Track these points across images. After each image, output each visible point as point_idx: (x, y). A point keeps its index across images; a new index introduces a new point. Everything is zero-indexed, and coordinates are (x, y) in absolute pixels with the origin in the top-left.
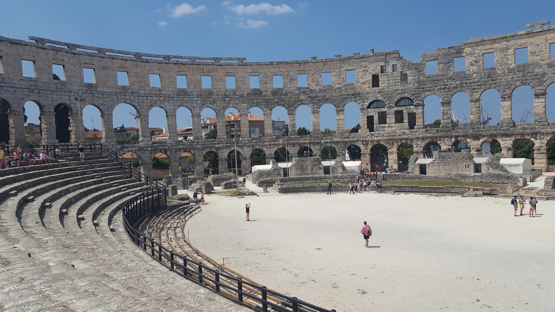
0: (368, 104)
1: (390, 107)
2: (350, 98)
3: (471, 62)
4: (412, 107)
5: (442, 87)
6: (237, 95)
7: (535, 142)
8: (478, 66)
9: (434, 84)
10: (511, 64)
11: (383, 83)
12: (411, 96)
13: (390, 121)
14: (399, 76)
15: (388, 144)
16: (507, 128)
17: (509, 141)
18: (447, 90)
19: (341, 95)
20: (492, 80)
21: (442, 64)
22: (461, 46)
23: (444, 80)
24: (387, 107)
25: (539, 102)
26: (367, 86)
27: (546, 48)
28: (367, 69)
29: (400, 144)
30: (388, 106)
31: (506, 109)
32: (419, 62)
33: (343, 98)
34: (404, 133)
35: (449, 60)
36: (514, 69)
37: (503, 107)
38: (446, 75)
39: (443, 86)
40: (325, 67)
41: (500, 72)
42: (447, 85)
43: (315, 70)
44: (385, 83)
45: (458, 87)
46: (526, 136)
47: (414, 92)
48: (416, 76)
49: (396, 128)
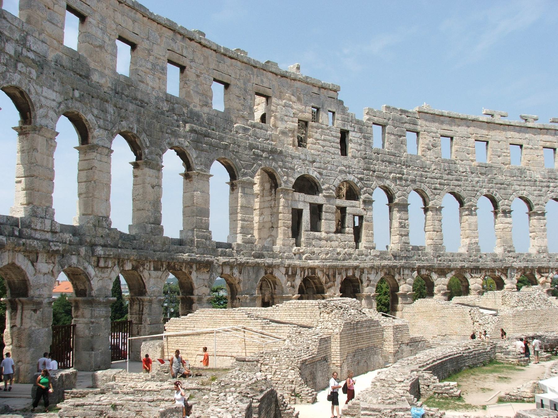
3: (428, 144)
6: (29, 50)
10: (472, 161)
11: (315, 144)
16: (476, 258)
17: (479, 279)
21: (393, 134)
24: (324, 196)
25: (507, 223)
29: (344, 277)
30: (325, 194)
33: (254, 154)
38: (398, 156)
39: (399, 174)
42: (403, 174)
43: (202, 64)
44: (319, 143)
46: (497, 272)
49: (337, 243)
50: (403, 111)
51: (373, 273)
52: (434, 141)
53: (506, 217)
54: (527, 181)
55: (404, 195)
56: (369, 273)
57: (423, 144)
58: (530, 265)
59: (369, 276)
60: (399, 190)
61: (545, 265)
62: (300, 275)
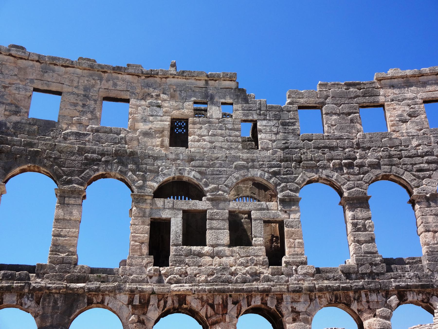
0: (156, 185)
2: (107, 162)
3: (401, 115)
4: (273, 205)
11: (198, 141)
12: (271, 178)
13: (218, 239)
15: (209, 308)
18: (358, 168)
19: (81, 151)
21: (335, 114)
23: (344, 148)
24: (208, 199)
26: (158, 141)
28: (160, 102)
30: (210, 196)
33: (86, 158)
38: (347, 139)
39: (345, 159)
40: (46, 75)
45: (382, 163)
47: (276, 169)
49: (232, 259)
51: (302, 300)
52: (412, 110)
56: (294, 301)
57: (390, 116)
59: (295, 305)
60: (349, 181)
62: (156, 305)
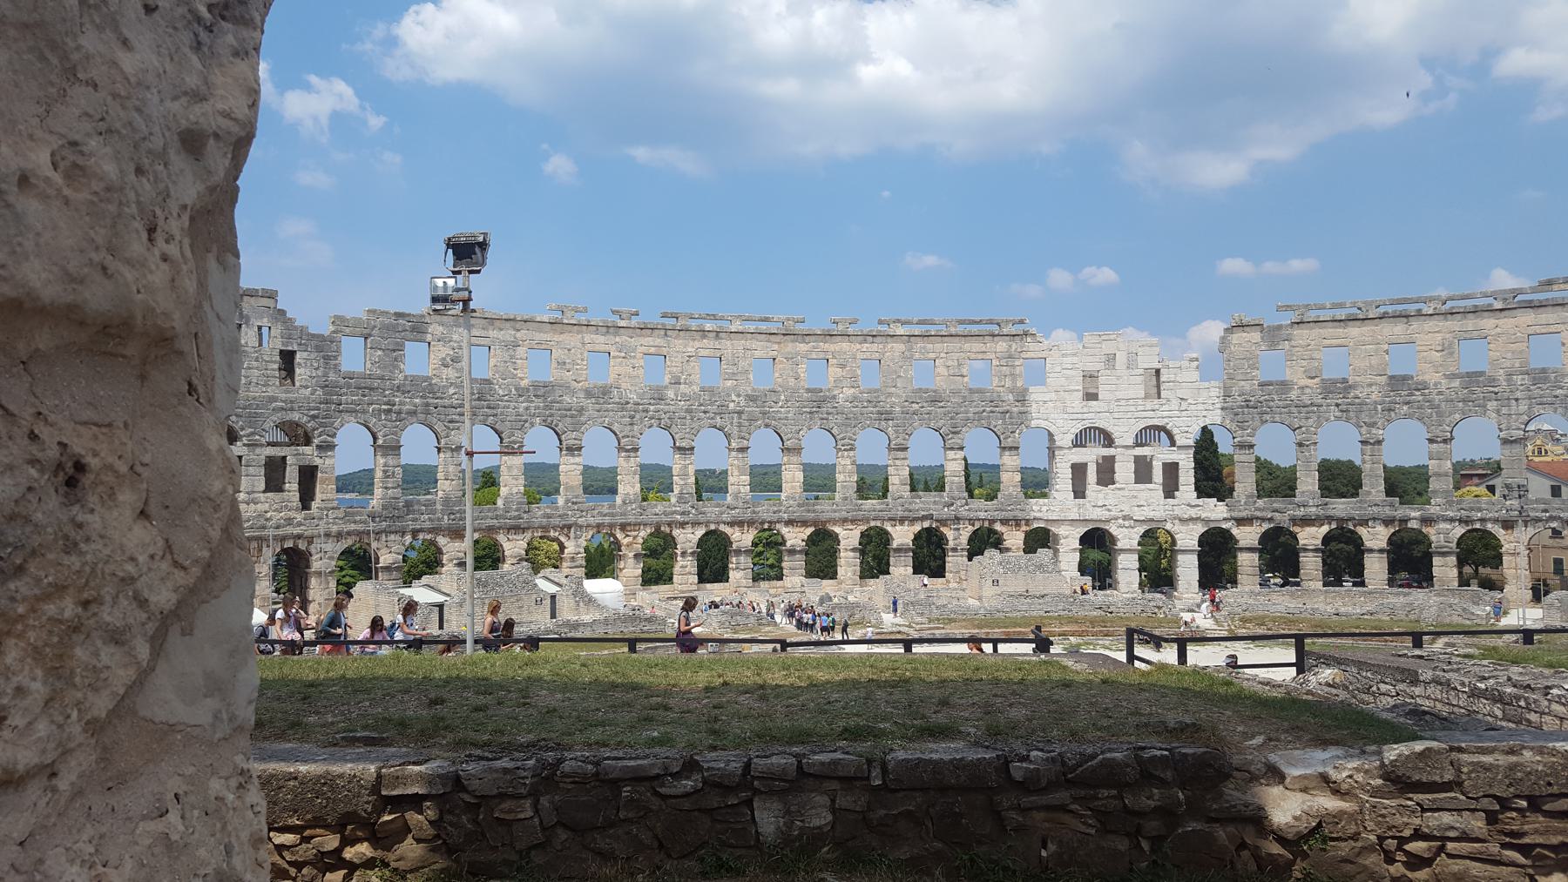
1: (252, 445)
3: (444, 359)
4: (307, 450)
5: (383, 407)
7: (566, 544)
8: (458, 370)
9: (364, 396)
10: (521, 379)
12: (309, 422)
14: (275, 362)
16: (517, 513)
20: (489, 408)
22: (423, 316)
23: (384, 390)
24: (244, 445)
27: (582, 360)
29: (278, 550)
30: (246, 442)
31: (515, 472)
32: (327, 333)
34: (290, 519)
35: (397, 343)
36: (528, 390)
37: (510, 468)
41: (501, 392)
42: (394, 405)
48: (316, 369)
49: (267, 505)
50: (399, 315)
53: (573, 455)
54: (613, 403)
55: (395, 434)
58: (607, 520)
61: (631, 519)
